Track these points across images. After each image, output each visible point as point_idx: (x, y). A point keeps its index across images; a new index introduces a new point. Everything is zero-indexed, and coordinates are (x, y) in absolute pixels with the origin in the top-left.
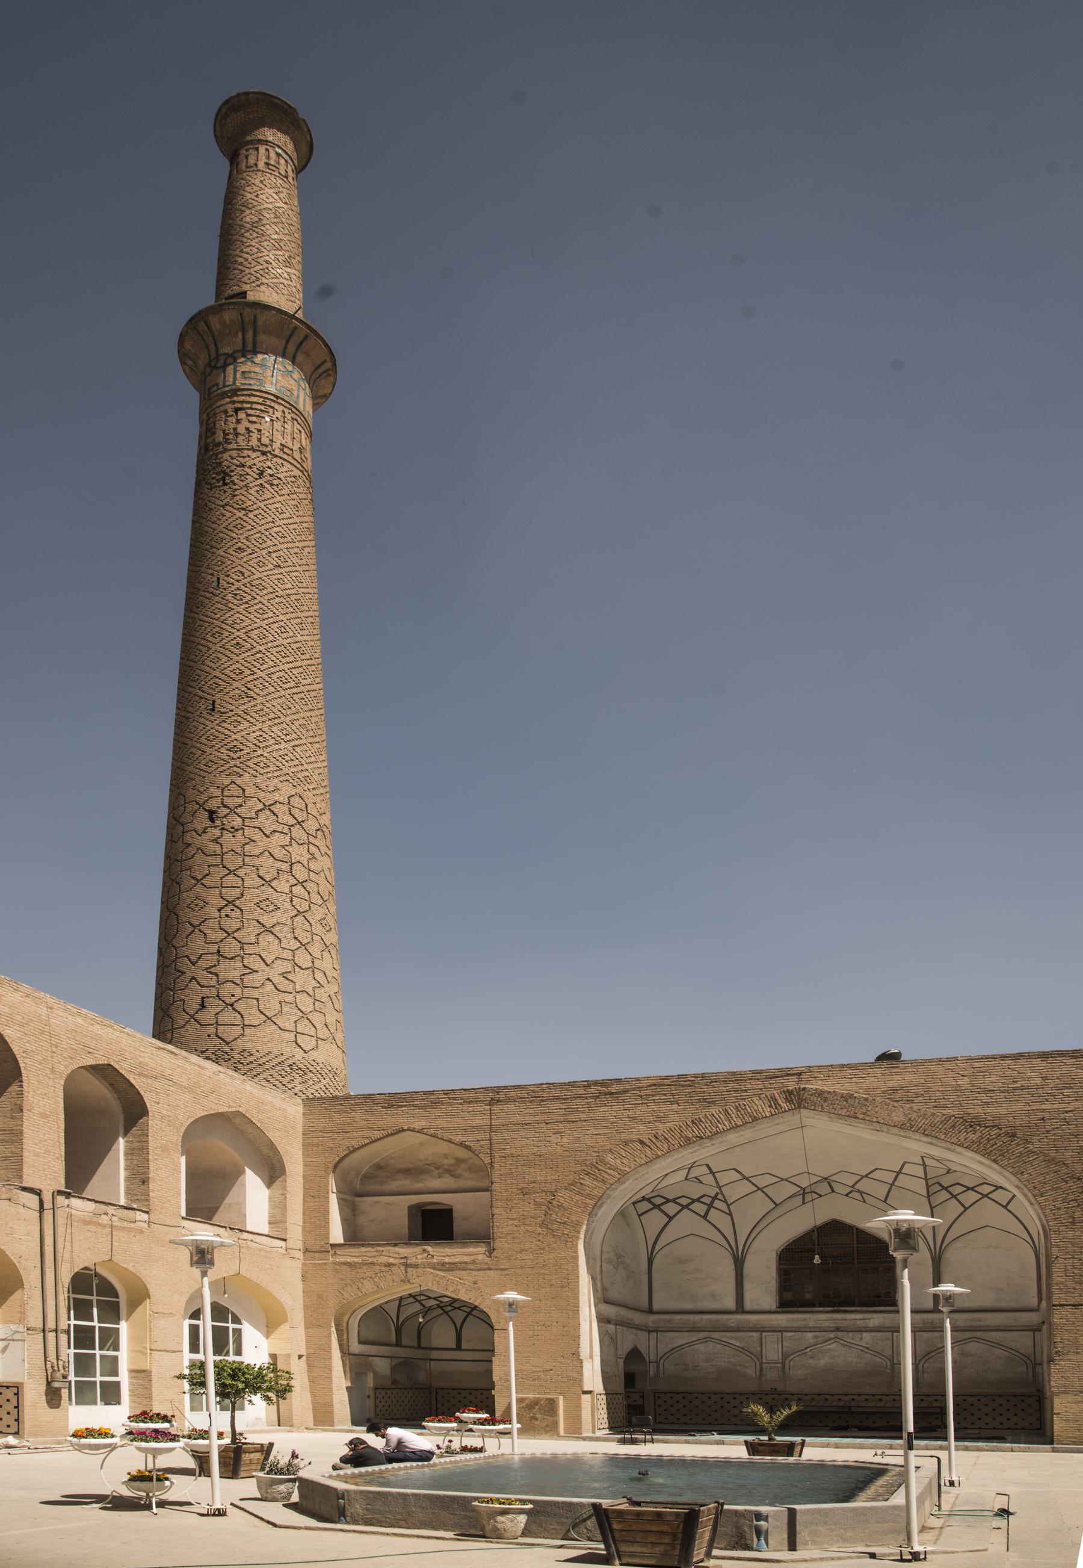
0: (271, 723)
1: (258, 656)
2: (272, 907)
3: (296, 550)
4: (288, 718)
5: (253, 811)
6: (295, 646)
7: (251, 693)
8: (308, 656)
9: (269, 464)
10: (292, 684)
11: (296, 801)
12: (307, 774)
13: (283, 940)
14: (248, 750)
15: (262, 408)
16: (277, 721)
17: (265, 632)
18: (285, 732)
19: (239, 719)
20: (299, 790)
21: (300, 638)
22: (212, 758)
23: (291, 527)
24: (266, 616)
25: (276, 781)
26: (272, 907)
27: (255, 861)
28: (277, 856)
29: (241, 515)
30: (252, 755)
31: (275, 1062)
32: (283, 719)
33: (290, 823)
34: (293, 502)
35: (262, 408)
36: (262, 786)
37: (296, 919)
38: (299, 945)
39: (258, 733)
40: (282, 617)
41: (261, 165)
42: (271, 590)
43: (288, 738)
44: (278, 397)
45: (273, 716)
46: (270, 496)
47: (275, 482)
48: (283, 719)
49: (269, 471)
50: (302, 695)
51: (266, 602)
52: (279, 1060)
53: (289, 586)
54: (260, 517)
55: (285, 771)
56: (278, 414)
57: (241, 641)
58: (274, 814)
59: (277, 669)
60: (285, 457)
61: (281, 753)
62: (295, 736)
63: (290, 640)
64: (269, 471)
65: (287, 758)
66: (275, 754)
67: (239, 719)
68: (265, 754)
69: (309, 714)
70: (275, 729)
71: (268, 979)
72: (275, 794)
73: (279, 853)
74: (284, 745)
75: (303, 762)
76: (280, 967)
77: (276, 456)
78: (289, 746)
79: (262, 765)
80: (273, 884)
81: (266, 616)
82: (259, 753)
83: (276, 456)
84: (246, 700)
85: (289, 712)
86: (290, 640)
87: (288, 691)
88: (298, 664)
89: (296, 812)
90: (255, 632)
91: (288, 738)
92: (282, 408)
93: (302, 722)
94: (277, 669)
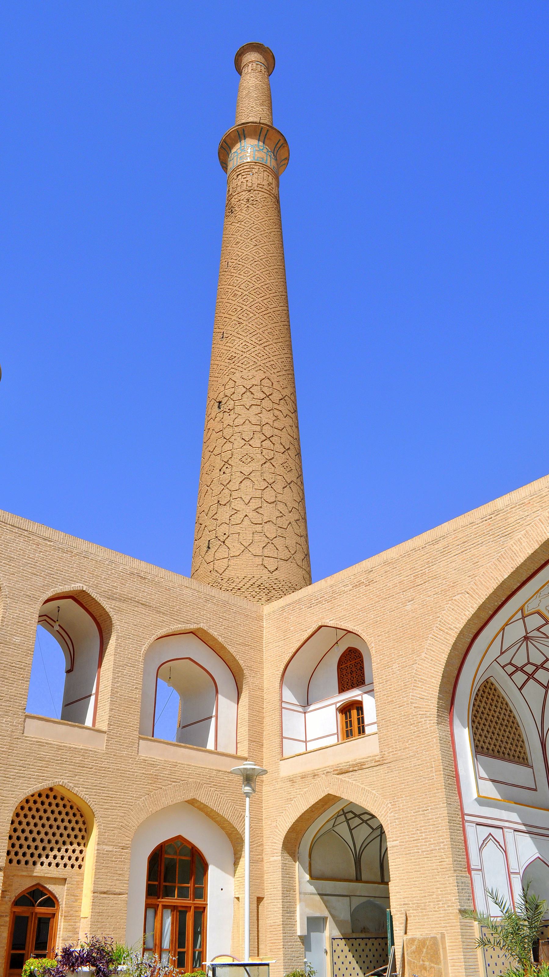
0: (251, 335)
1: (245, 297)
2: (249, 460)
3: (266, 235)
4: (261, 330)
5: (240, 395)
6: (265, 287)
7: (241, 321)
8: (273, 291)
9: (252, 195)
10: (264, 309)
11: (266, 382)
12: (272, 363)
13: (256, 482)
14: (238, 356)
15: (249, 170)
16: (254, 333)
17: (249, 283)
18: (259, 339)
19: (234, 338)
20: (267, 374)
21: (268, 281)
22: (221, 367)
23: (263, 223)
24: (249, 274)
25: (254, 371)
26: (249, 460)
27: (240, 429)
28: (253, 422)
29: (238, 225)
30: (241, 358)
31: (248, 585)
32: (258, 331)
33: (262, 398)
34: (264, 211)
35: (249, 170)
36: (245, 377)
37: (264, 466)
38: (266, 484)
39: (244, 344)
40: (258, 272)
41: (250, 71)
42: (252, 259)
43: (261, 342)
44: (256, 163)
45: (252, 331)
46: (252, 210)
47: (255, 203)
48: (258, 331)
49: (252, 199)
50: (270, 314)
51: (249, 267)
52: (251, 582)
53: (262, 254)
54: (247, 223)
55: (259, 363)
56: (256, 171)
57: (236, 292)
58: (252, 393)
59: (255, 302)
60: (260, 189)
61: (256, 353)
62: (265, 340)
63: (262, 284)
64: (252, 199)
65: (260, 355)
66: (253, 354)
67: (234, 338)
68: (248, 356)
69: (274, 325)
70: (253, 339)
71: (246, 515)
72: (253, 380)
73: (254, 420)
74: (258, 347)
75: (270, 356)
76: (254, 504)
77: (255, 190)
78: (261, 347)
79: (245, 363)
80: (251, 443)
81: (249, 274)
82: (244, 356)
83: (255, 190)
84: (238, 325)
85: (262, 326)
86: (262, 284)
87: (261, 314)
88: (267, 297)
89: (265, 390)
90: (244, 285)
91: (261, 342)
92: (258, 167)
93: (270, 330)
94: (255, 302)
